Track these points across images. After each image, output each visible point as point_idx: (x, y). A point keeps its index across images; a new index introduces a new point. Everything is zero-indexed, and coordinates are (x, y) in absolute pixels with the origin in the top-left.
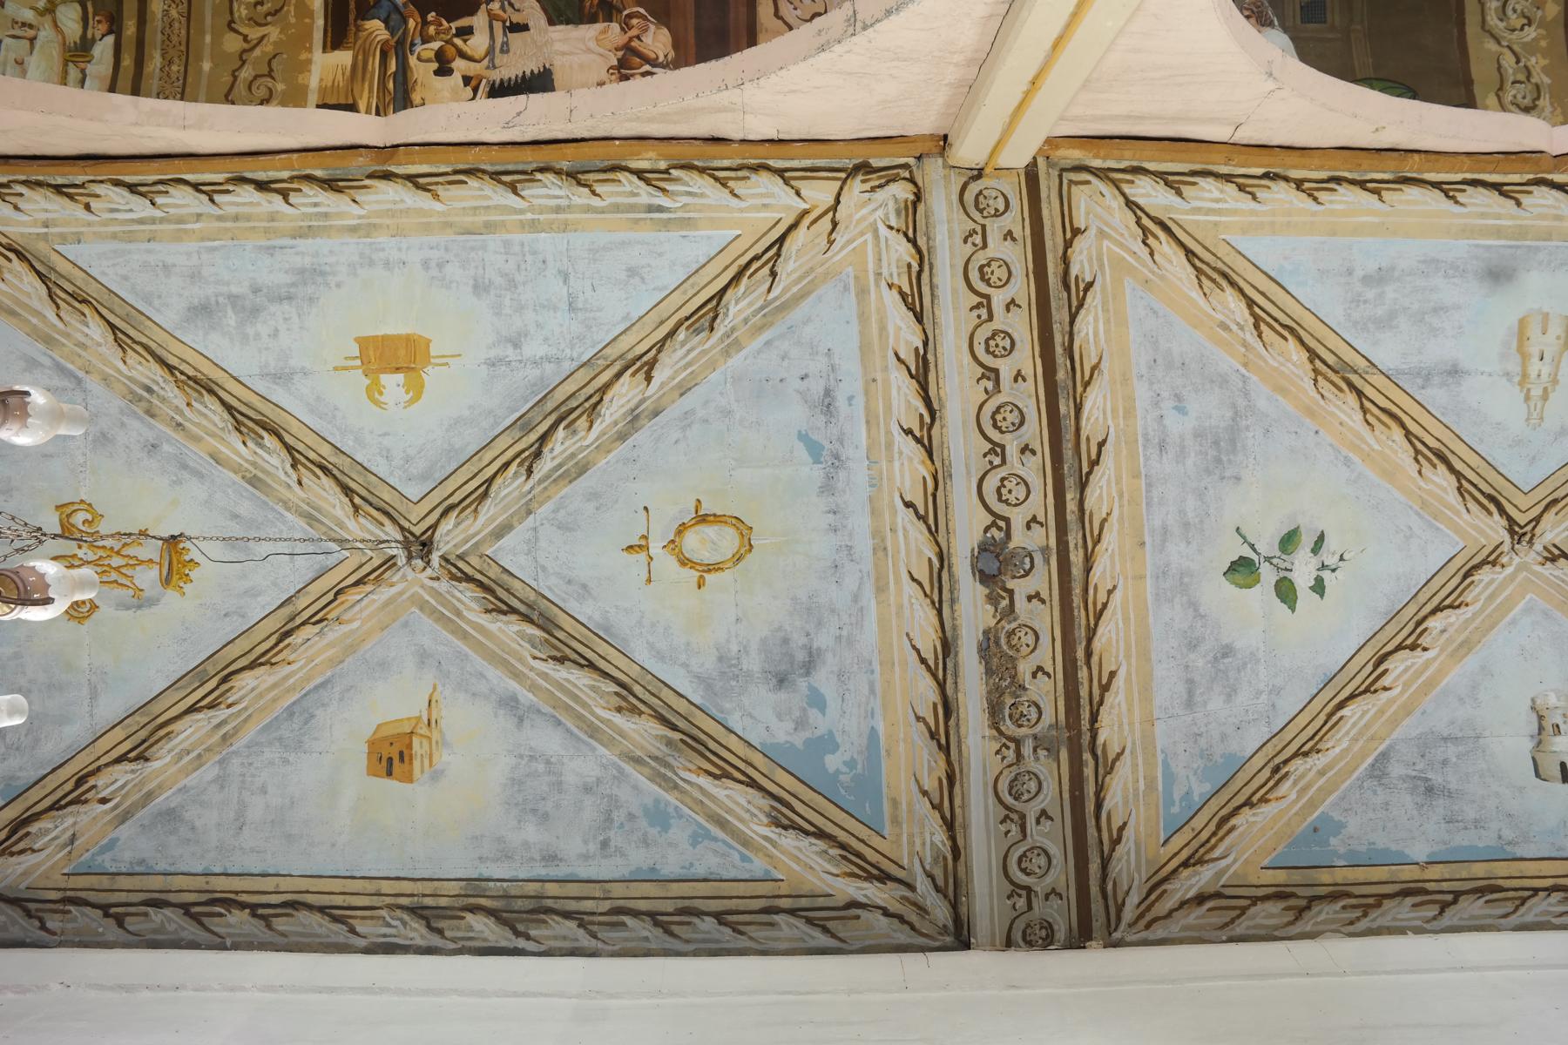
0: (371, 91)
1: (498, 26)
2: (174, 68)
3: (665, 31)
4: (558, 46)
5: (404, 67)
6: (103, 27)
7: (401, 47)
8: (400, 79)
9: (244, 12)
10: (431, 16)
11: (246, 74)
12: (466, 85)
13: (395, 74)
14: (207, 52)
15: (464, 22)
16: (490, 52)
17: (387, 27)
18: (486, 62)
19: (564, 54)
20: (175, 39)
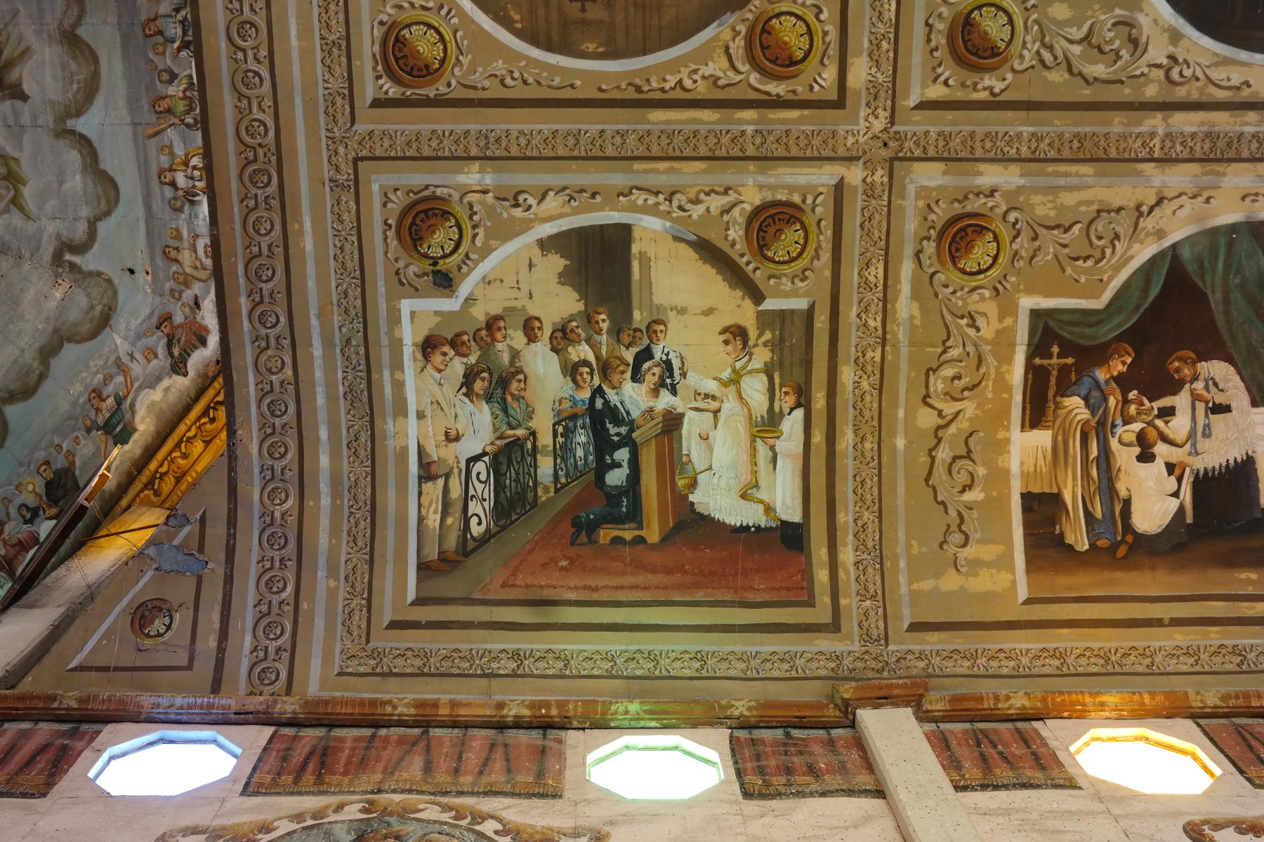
0: (1074, 478)
1: (1201, 407)
2: (868, 445)
5: (1105, 452)
6: (791, 400)
7: (1101, 428)
8: (1104, 466)
9: (940, 386)
10: (1133, 395)
11: (943, 454)
12: (1170, 474)
13: (1098, 458)
14: (900, 427)
15: (1165, 402)
16: (1192, 435)
17: (1087, 405)
20: (867, 413)
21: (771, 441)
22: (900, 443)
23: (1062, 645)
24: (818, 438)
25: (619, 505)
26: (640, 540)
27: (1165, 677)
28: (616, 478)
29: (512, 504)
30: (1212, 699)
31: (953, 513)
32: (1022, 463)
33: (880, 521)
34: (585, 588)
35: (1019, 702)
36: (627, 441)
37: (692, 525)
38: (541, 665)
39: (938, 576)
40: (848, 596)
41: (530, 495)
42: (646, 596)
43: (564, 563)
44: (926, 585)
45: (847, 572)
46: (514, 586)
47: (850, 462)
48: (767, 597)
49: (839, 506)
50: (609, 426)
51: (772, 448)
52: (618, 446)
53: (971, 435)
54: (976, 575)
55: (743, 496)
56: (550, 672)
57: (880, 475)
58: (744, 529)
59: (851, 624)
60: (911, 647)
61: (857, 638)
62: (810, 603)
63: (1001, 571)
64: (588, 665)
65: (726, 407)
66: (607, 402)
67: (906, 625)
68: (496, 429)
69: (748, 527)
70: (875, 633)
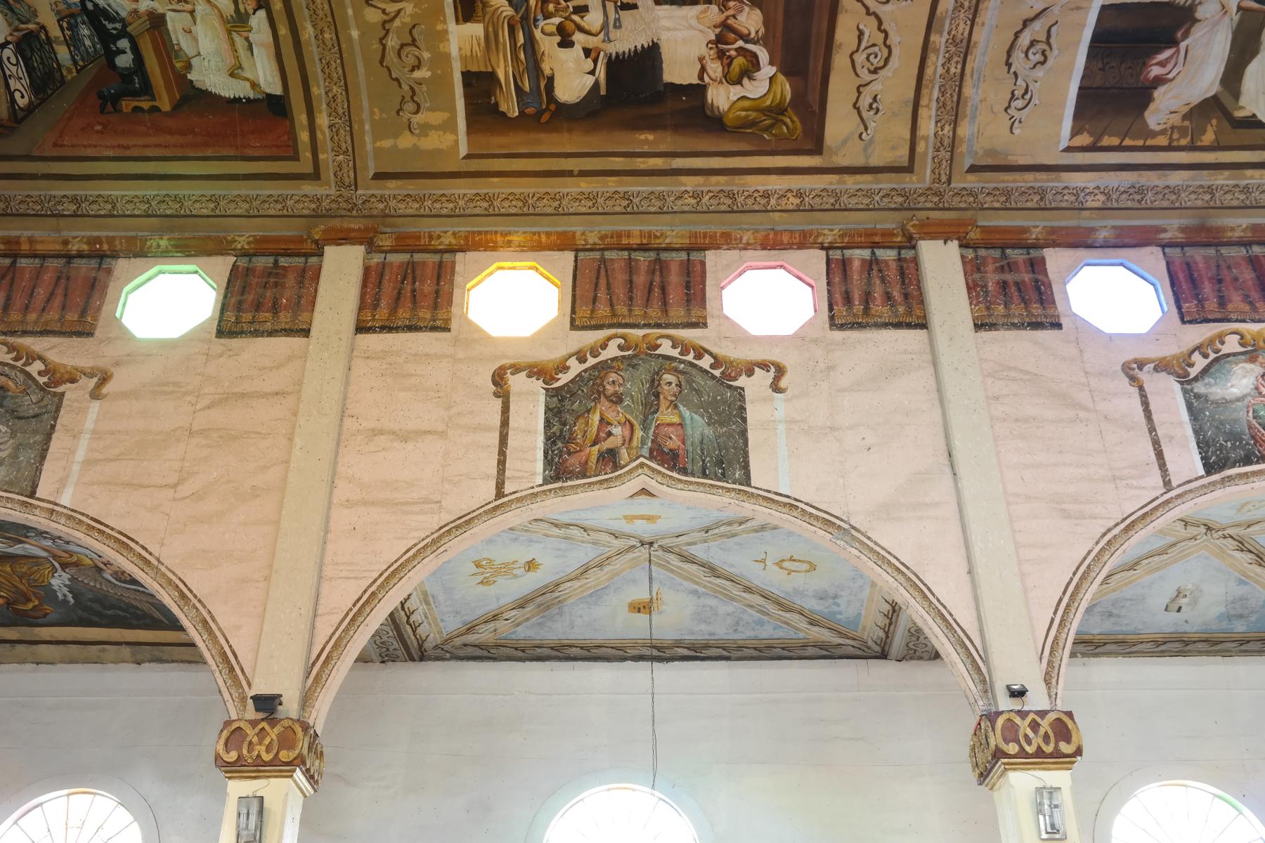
1: (610, 6)
2: (327, 36)
3: (758, 12)
4: (664, 23)
5: (530, 39)
11: (392, 42)
13: (524, 45)
14: (352, 22)
16: (605, 26)
18: (601, 36)
19: (669, 29)
20: (320, 13)
21: (245, 34)
22: (355, 34)
23: (491, 191)
24: (283, 31)
25: (132, 82)
26: (155, 109)
27: (566, 217)
28: (125, 61)
29: (45, 81)
30: (593, 239)
31: (406, 88)
32: (460, 49)
33: (347, 93)
34: (119, 146)
35: (448, 240)
36: (124, 33)
37: (195, 99)
38: (95, 207)
39: (396, 135)
40: (325, 152)
41: (57, 75)
42: (167, 153)
43: (99, 128)
44: (387, 143)
45: (323, 133)
46: (62, 146)
47: (315, 49)
48: (261, 153)
49: (311, 82)
50: (106, 23)
51: (247, 39)
52: (118, 37)
53: (414, 27)
54: (426, 135)
55: (232, 75)
56: (102, 213)
57: (341, 58)
58: (237, 100)
59: (328, 173)
60: (375, 192)
61: (333, 185)
62: (295, 157)
63: (448, 133)
64: (130, 206)
65: (199, 8)
66: (96, 5)
67: (371, 174)
68: (10, 25)
69: (240, 99)
70: (347, 181)
